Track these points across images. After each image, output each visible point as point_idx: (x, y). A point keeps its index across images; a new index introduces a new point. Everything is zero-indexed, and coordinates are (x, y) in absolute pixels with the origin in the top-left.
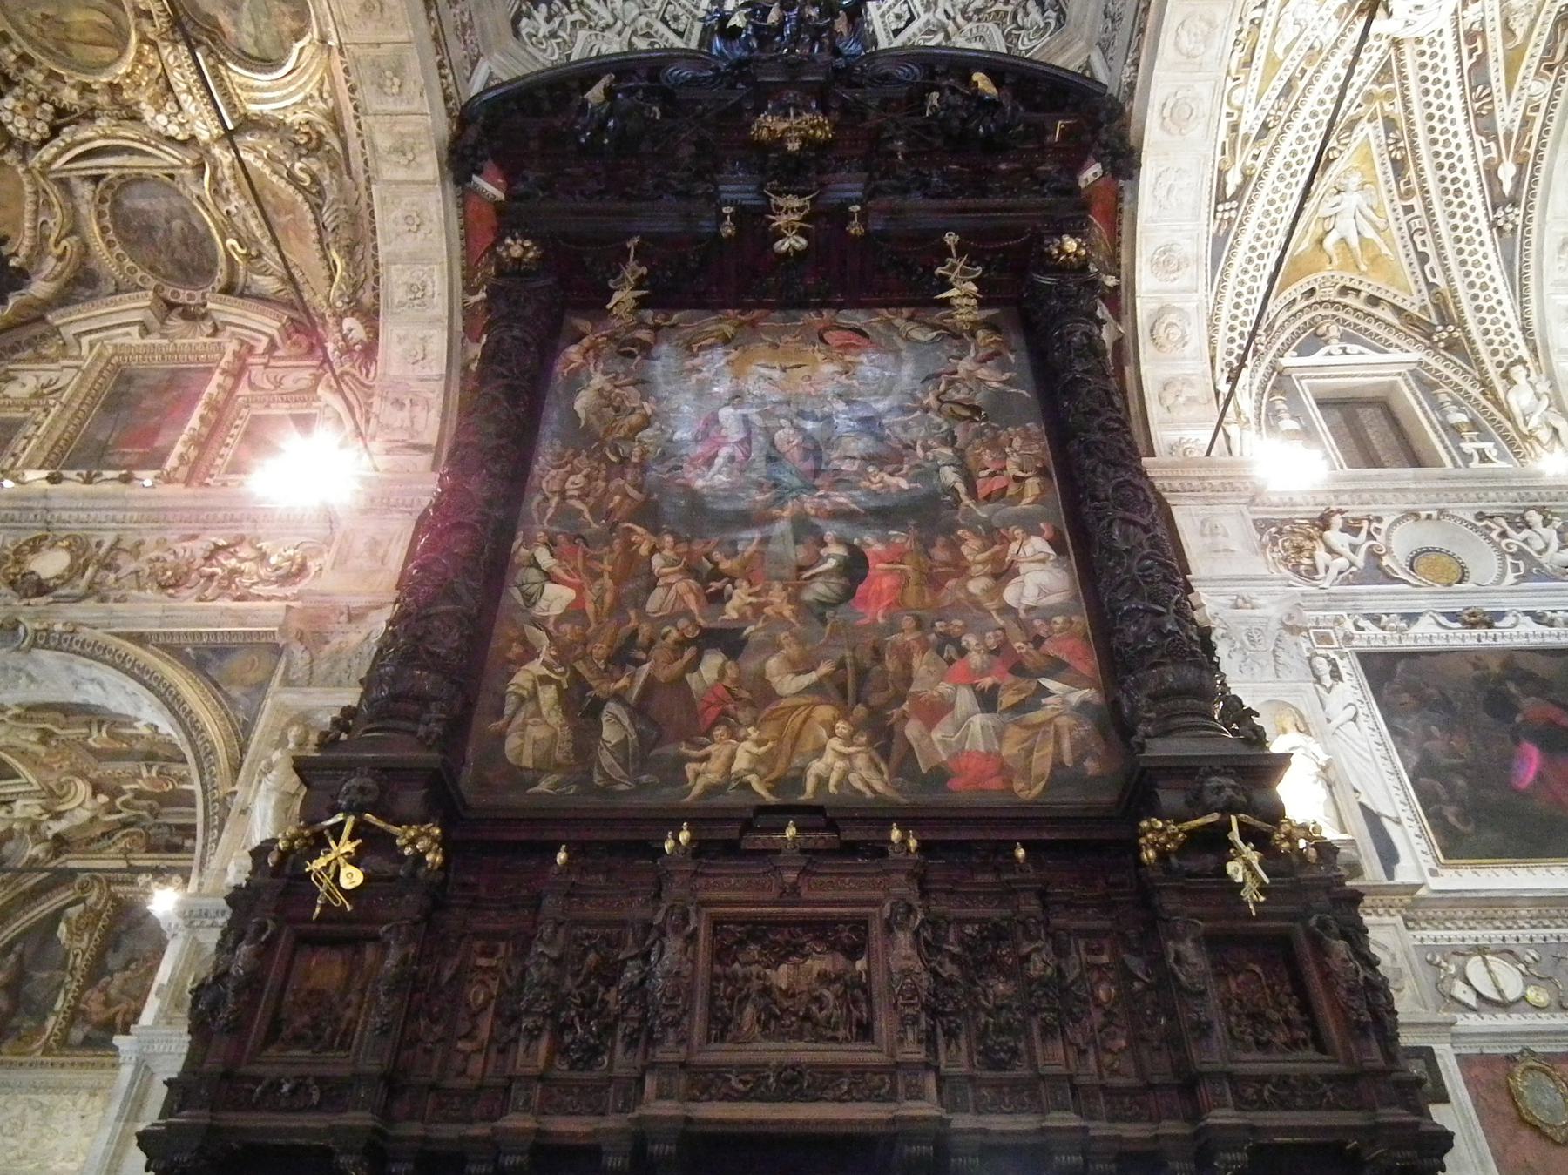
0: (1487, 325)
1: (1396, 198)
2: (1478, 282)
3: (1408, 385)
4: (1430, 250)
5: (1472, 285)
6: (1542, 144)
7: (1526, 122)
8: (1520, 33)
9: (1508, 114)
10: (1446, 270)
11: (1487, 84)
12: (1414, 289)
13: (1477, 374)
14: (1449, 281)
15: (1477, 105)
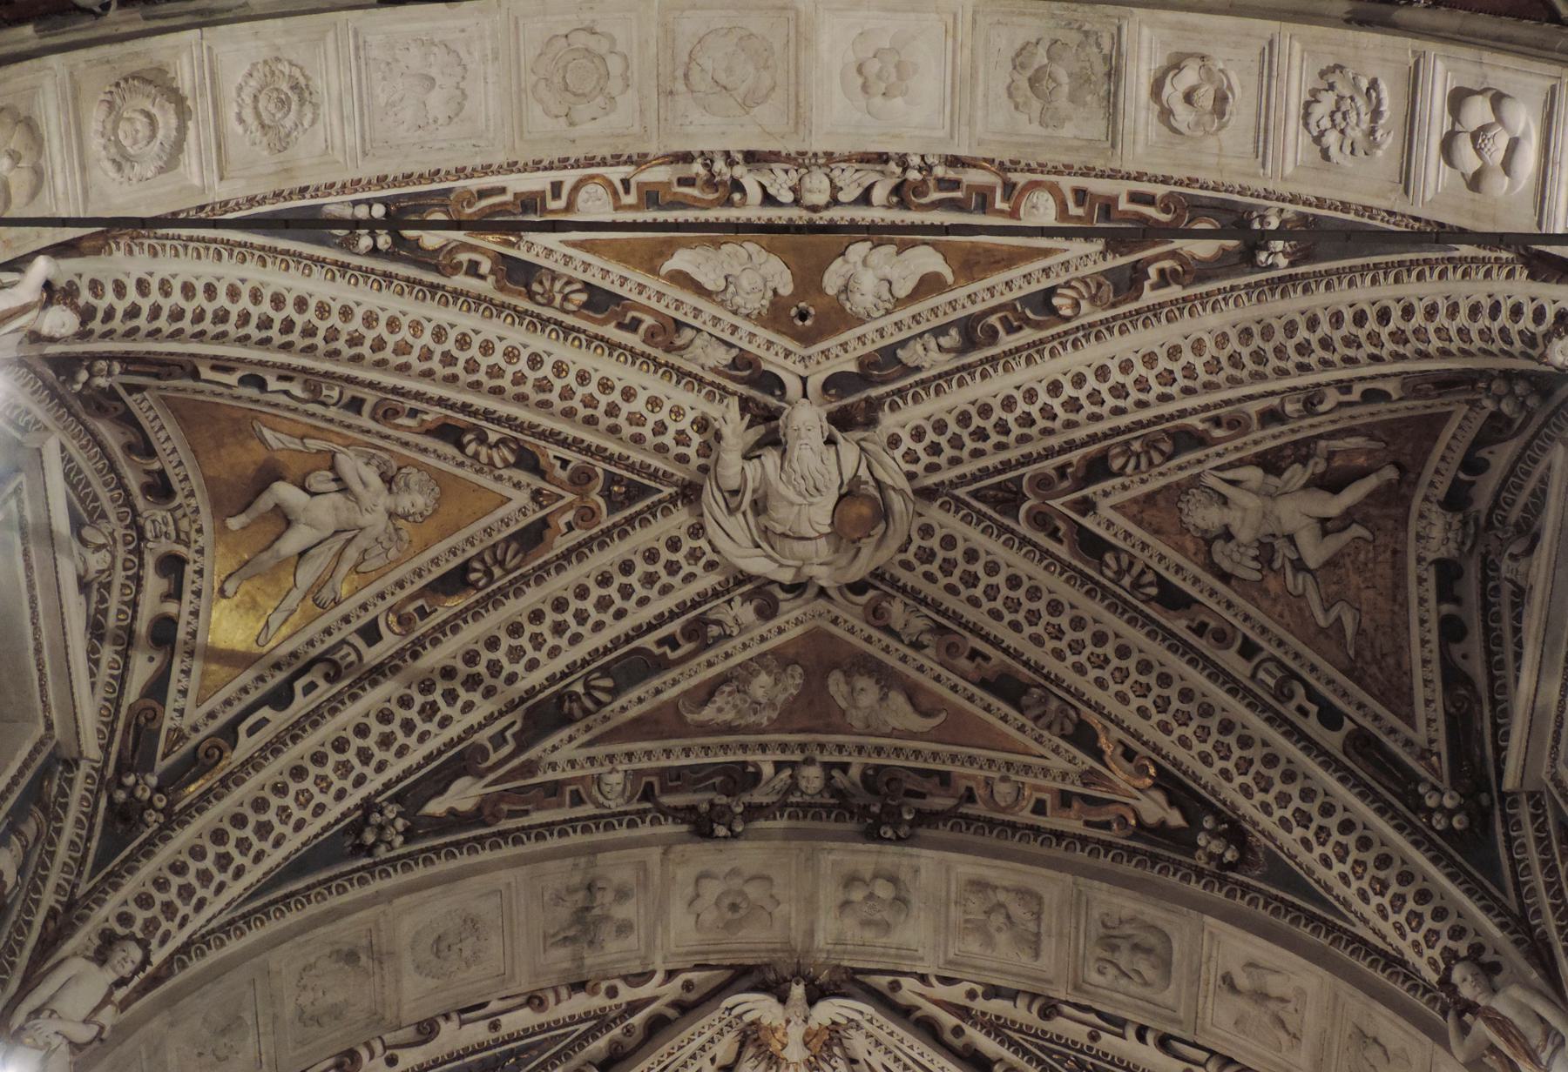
0: (194, 866)
1: (390, 601)
2: (271, 816)
3: (36, 750)
4: (301, 704)
5: (260, 805)
6: (515, 836)
7: (554, 789)
8: (708, 713)
9: (568, 752)
10: (274, 748)
11: (614, 692)
12: (214, 703)
13: (84, 888)
14: (253, 764)
15: (579, 688)
